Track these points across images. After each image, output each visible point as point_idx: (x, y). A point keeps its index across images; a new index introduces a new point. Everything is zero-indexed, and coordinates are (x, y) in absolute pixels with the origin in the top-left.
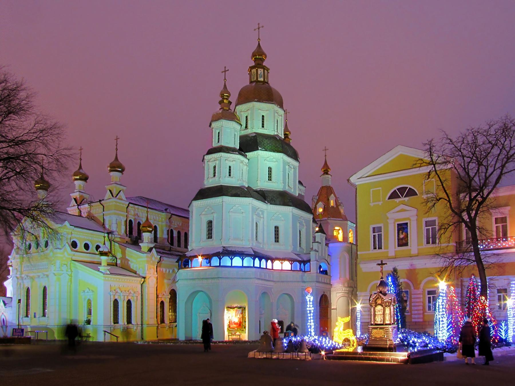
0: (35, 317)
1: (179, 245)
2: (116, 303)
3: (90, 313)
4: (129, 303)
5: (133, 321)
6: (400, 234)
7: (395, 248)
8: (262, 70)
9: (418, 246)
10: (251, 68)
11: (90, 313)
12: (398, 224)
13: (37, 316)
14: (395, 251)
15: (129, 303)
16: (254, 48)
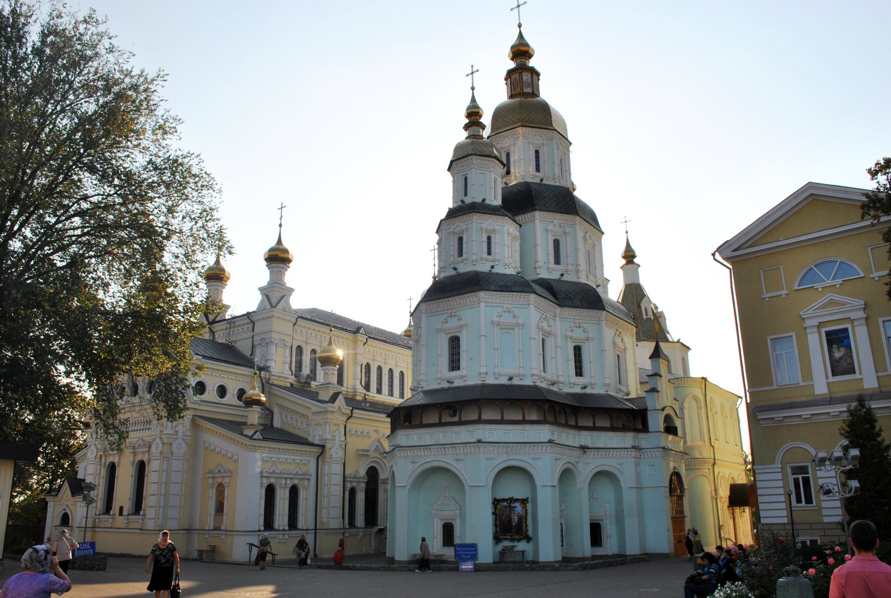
0: (121, 514)
1: (379, 391)
2: (270, 491)
3: (220, 508)
4: (294, 492)
5: (300, 524)
6: (835, 350)
7: (827, 378)
8: (529, 75)
9: (876, 372)
10: (510, 73)
11: (220, 508)
12: (828, 334)
13: (125, 512)
14: (829, 384)
15: (294, 492)
16: (513, 40)
